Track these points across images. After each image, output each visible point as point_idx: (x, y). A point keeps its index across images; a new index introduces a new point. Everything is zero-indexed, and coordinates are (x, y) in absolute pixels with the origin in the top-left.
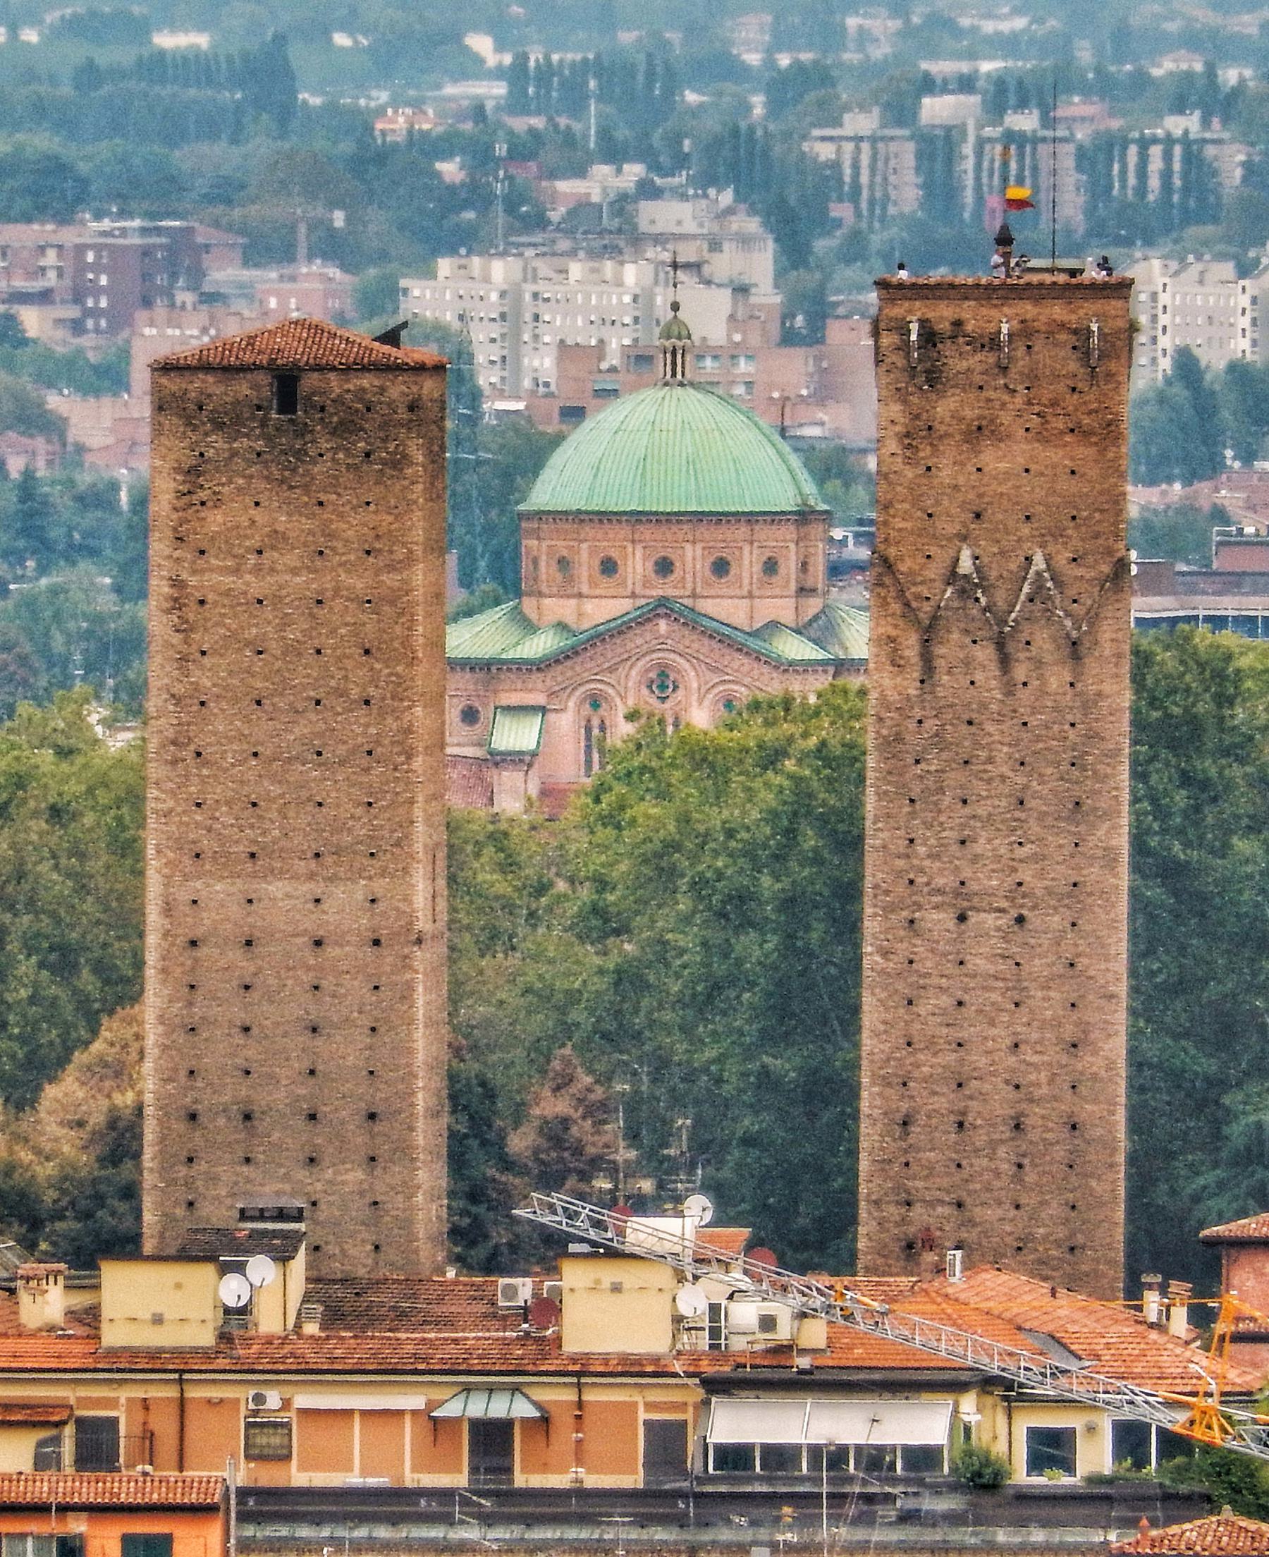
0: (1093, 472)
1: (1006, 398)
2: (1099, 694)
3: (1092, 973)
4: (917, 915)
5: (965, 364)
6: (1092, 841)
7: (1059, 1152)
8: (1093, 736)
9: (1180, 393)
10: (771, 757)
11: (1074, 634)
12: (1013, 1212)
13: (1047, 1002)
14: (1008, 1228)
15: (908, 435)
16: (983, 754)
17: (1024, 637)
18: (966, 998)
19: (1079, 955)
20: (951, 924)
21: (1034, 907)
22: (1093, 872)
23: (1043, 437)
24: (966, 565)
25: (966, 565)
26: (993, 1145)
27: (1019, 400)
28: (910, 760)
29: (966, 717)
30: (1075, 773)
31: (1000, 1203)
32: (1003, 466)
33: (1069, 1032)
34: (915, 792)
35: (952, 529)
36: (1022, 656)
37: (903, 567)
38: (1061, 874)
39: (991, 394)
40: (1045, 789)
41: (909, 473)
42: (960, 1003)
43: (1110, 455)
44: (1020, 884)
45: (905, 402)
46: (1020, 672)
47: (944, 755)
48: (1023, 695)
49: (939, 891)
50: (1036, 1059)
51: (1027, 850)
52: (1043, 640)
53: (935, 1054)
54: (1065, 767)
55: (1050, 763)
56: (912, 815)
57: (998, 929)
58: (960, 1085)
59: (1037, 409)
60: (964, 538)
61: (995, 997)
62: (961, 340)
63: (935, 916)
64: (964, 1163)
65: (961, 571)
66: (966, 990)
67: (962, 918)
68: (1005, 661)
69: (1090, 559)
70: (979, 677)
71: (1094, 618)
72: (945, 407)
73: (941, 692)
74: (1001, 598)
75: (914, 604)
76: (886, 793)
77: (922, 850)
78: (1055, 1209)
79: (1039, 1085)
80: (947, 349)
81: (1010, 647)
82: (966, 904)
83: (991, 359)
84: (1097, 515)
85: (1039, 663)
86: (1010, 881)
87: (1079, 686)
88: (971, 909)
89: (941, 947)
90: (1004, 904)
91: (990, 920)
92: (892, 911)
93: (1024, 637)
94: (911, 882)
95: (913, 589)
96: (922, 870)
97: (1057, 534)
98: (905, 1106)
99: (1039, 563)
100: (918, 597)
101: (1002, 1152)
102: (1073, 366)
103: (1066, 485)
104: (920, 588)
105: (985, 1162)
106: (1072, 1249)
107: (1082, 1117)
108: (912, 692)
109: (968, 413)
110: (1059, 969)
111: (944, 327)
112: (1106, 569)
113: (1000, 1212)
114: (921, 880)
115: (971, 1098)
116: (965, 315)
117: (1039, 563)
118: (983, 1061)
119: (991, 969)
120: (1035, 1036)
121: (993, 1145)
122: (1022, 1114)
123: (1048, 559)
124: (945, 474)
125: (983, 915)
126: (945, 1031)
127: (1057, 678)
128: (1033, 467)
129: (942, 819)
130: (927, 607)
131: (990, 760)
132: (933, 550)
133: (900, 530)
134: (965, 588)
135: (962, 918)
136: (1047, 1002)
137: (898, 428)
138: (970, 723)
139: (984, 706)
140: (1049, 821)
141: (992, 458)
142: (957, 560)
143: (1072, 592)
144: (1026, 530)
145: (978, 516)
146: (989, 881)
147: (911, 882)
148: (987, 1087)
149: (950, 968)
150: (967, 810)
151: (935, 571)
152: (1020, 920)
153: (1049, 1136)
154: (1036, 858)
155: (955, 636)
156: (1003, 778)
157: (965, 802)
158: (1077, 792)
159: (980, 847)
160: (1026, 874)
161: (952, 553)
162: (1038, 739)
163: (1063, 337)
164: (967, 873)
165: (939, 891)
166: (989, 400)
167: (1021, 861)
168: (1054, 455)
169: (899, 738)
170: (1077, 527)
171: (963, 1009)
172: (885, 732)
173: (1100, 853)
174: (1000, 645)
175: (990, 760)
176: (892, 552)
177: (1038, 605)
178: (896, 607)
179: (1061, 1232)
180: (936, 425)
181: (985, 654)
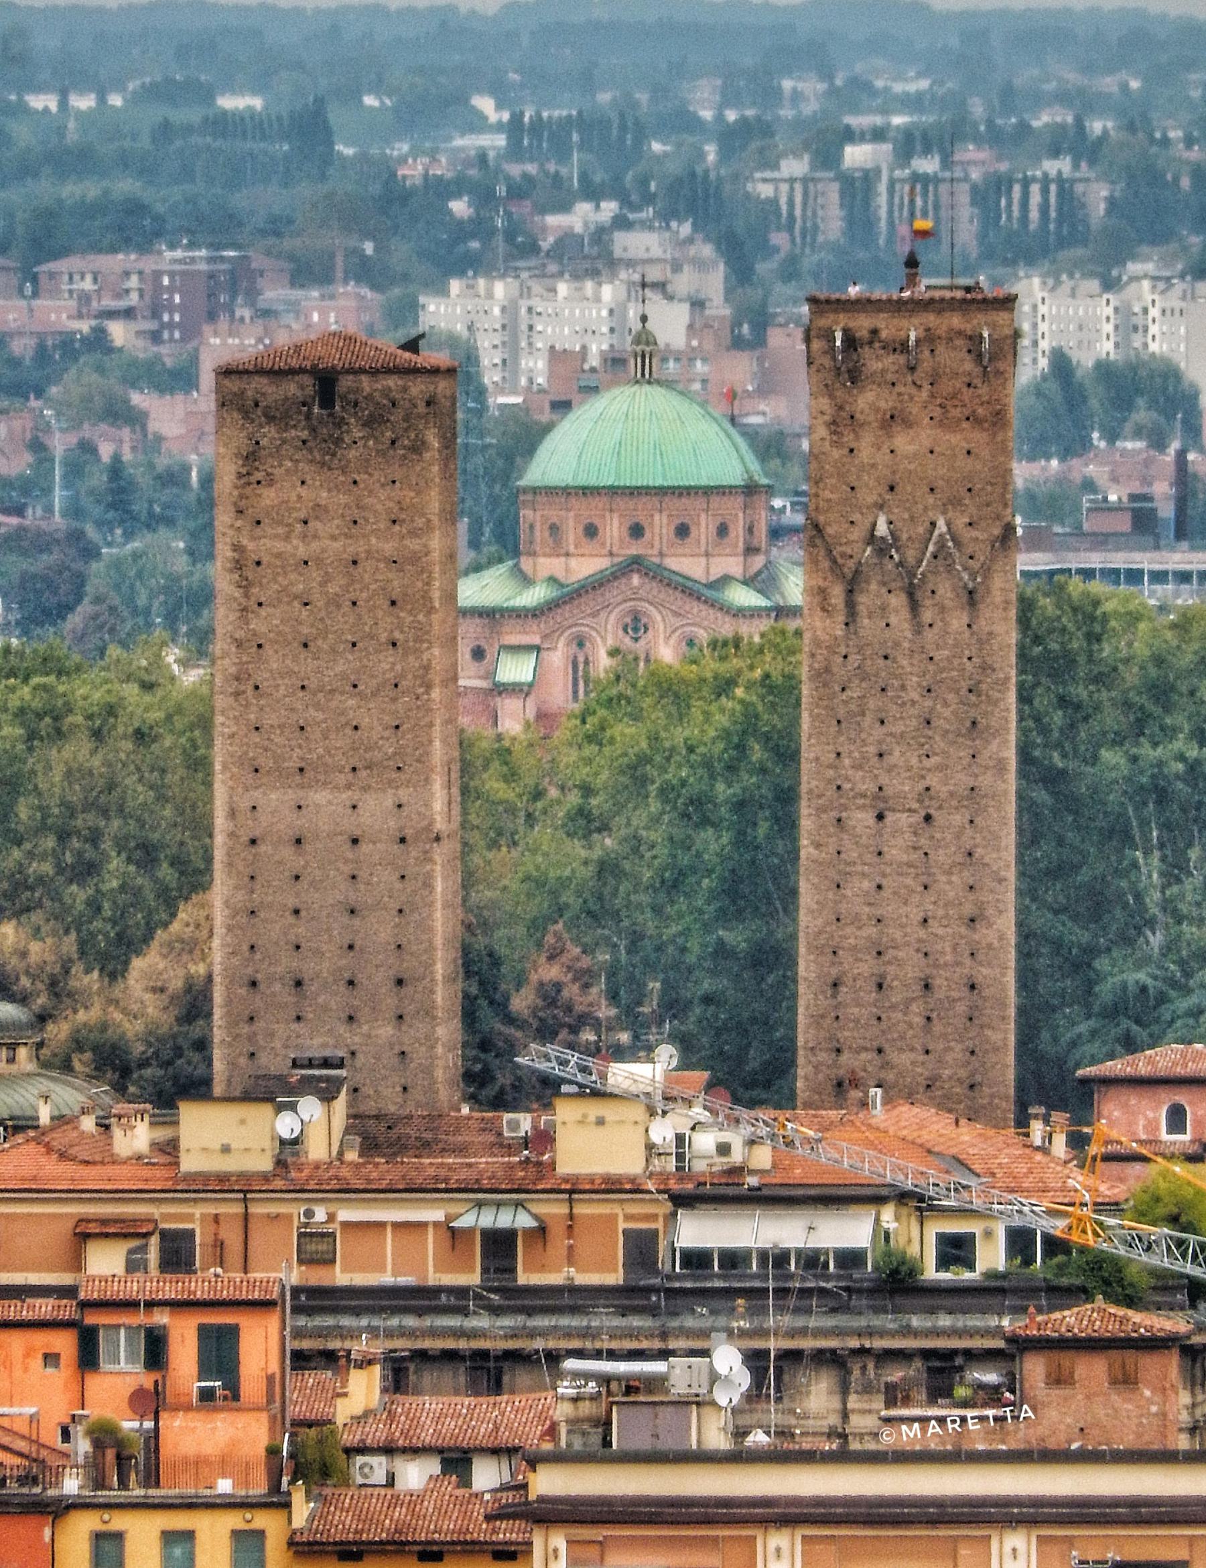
0: (985, 453)
1: (914, 391)
2: (990, 633)
3: (986, 860)
4: (844, 814)
5: (880, 365)
6: (986, 754)
7: (961, 1008)
8: (986, 668)
9: (1053, 387)
10: (724, 686)
11: (971, 585)
12: (922, 1058)
13: (951, 886)
14: (919, 1070)
15: (834, 422)
16: (896, 683)
17: (930, 586)
18: (884, 882)
19: (976, 846)
20: (871, 821)
21: (940, 808)
22: (986, 781)
23: (944, 423)
24: (882, 529)
25: (882, 529)
26: (908, 1002)
27: (924, 394)
28: (837, 688)
29: (882, 653)
30: (973, 698)
31: (912, 1049)
32: (911, 448)
33: (968, 910)
34: (841, 712)
35: (871, 499)
36: (928, 602)
37: (830, 530)
38: (962, 780)
39: (902, 389)
40: (946, 714)
41: (836, 454)
42: (879, 887)
43: (999, 439)
44: (928, 789)
45: (831, 396)
46: (927, 616)
47: (864, 685)
48: (929, 635)
49: (864, 796)
50: (940, 931)
51: (934, 760)
52: (945, 590)
53: (860, 928)
54: (964, 692)
55: (951, 690)
56: (839, 732)
58: (879, 953)
59: (938, 401)
60: (881, 507)
61: (909, 881)
62: (877, 345)
63: (860, 815)
64: (883, 1016)
65: (877, 533)
66: (884, 875)
67: (880, 817)
68: (914, 606)
69: (983, 524)
70: (893, 620)
71: (987, 571)
72: (867, 401)
73: (862, 633)
74: (911, 555)
75: (840, 561)
76: (818, 715)
77: (847, 762)
78: (957, 1052)
79: (943, 953)
80: (866, 352)
81: (919, 595)
82: (882, 805)
83: (902, 359)
84: (989, 488)
85: (943, 609)
86: (920, 787)
87: (974, 627)
88: (889, 809)
89: (864, 840)
90: (915, 806)
91: (904, 819)
92: (825, 811)
93: (930, 586)
94: (839, 788)
95: (840, 549)
96: (848, 779)
97: (954, 502)
98: (834, 971)
99: (941, 526)
100: (843, 555)
101: (914, 1007)
102: (969, 366)
103: (962, 462)
104: (843, 549)
105: (900, 1015)
106: (972, 1087)
107: (979, 980)
108: (839, 633)
109: (882, 404)
110: (960, 858)
111: (863, 334)
112: (997, 531)
113: (912, 1056)
115: (889, 963)
116: (881, 325)
117: (941, 526)
118: (898, 935)
119: (905, 858)
120: (941, 912)
121: (908, 1002)
122: (928, 977)
123: (948, 524)
124: (865, 452)
125: (898, 815)
126: (867, 909)
127: (958, 621)
128: (937, 449)
129: (863, 736)
130: (851, 564)
132: (856, 517)
133: (829, 501)
134: (882, 548)
135: (880, 817)
136: (951, 886)
137: (827, 418)
138: (886, 657)
139: (897, 644)
140: (951, 736)
141: (903, 442)
142: (874, 524)
143: (969, 551)
144: (931, 500)
145: (892, 488)
146: (901, 786)
148: (901, 954)
149: (869, 858)
150: (884, 730)
151: (857, 534)
152: (928, 818)
154: (940, 768)
155: (873, 586)
156: (913, 703)
157: (882, 722)
158: (973, 713)
159: (895, 757)
160: (933, 780)
161: (871, 519)
162: (942, 671)
163: (959, 342)
164: (884, 780)
165: (864, 796)
166: (899, 394)
167: (929, 770)
168: (955, 439)
169: (827, 670)
170: (972, 498)
172: (816, 665)
174: (911, 595)
175: (903, 687)
176: (821, 519)
177: (940, 561)
178: (826, 564)
179: (963, 1073)
180: (858, 416)
181: (898, 601)
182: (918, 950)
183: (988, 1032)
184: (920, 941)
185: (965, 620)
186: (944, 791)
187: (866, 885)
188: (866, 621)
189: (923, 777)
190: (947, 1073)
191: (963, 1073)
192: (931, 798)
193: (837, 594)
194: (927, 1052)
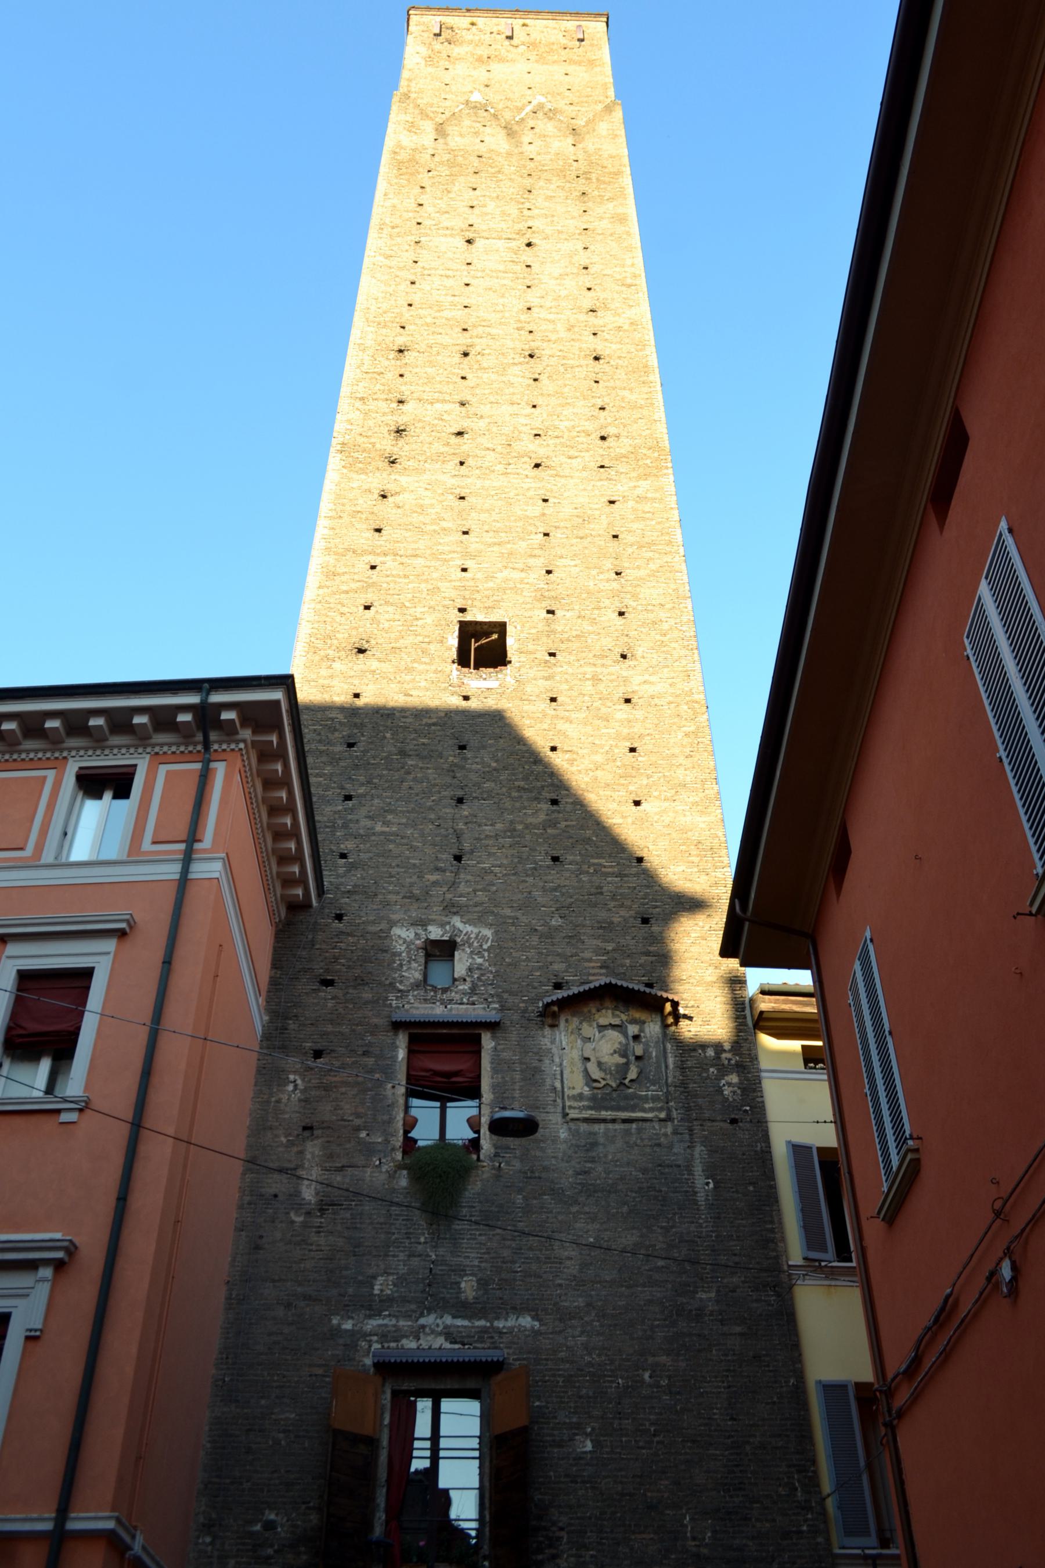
23: (541, 59)
33: (588, 304)
46: (526, 139)
50: (552, 317)
51: (535, 212)
53: (439, 311)
57: (509, 248)
86: (523, 226)
105: (494, 377)
114: (426, 222)
119: (502, 268)
120: (548, 304)
127: (563, 144)
131: (499, 172)
147: (419, 224)
148: (493, 331)
153: (571, 362)
155: (467, 122)
159: (491, 206)
171: (469, 288)
173: (607, 215)
182: (518, 329)
183: (626, 393)
184: (519, 321)
185: (570, 140)
186: (549, 230)
187: (449, 282)
188: (458, 139)
189: (526, 221)
190: (563, 425)
191: (589, 426)
192: (534, 232)
193: (428, 127)
194: (534, 406)
